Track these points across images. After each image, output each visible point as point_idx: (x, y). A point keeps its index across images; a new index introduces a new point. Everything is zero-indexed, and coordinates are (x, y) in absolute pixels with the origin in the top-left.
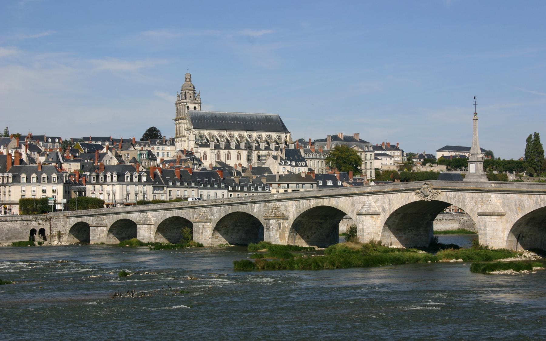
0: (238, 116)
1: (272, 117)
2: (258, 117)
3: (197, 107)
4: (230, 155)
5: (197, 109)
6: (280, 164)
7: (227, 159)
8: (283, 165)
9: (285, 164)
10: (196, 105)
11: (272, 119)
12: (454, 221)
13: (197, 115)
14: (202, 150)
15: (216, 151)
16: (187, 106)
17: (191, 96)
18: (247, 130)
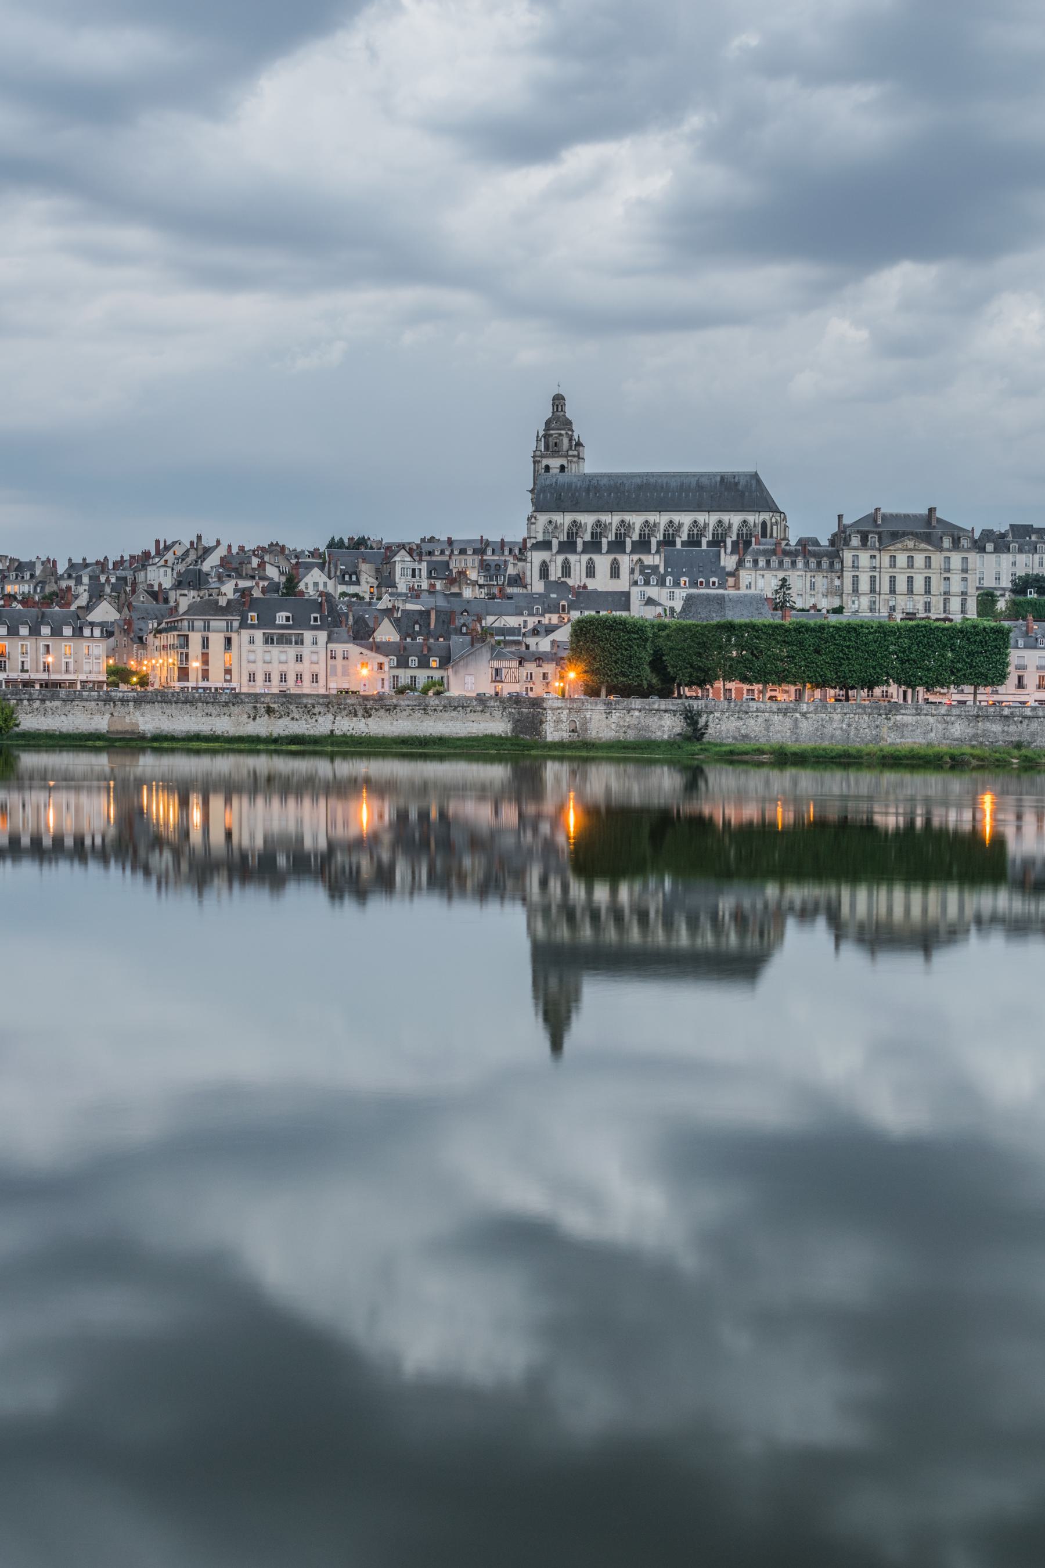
0: (652, 480)
1: (737, 479)
2: (704, 481)
3: (566, 466)
4: (594, 567)
5: (566, 470)
6: (636, 583)
7: (587, 577)
8: (641, 586)
9: (647, 583)
10: (564, 462)
11: (737, 484)
12: (488, 714)
13: (556, 483)
14: (537, 557)
15: (560, 558)
16: (545, 462)
17: (556, 443)
18: (660, 508)
